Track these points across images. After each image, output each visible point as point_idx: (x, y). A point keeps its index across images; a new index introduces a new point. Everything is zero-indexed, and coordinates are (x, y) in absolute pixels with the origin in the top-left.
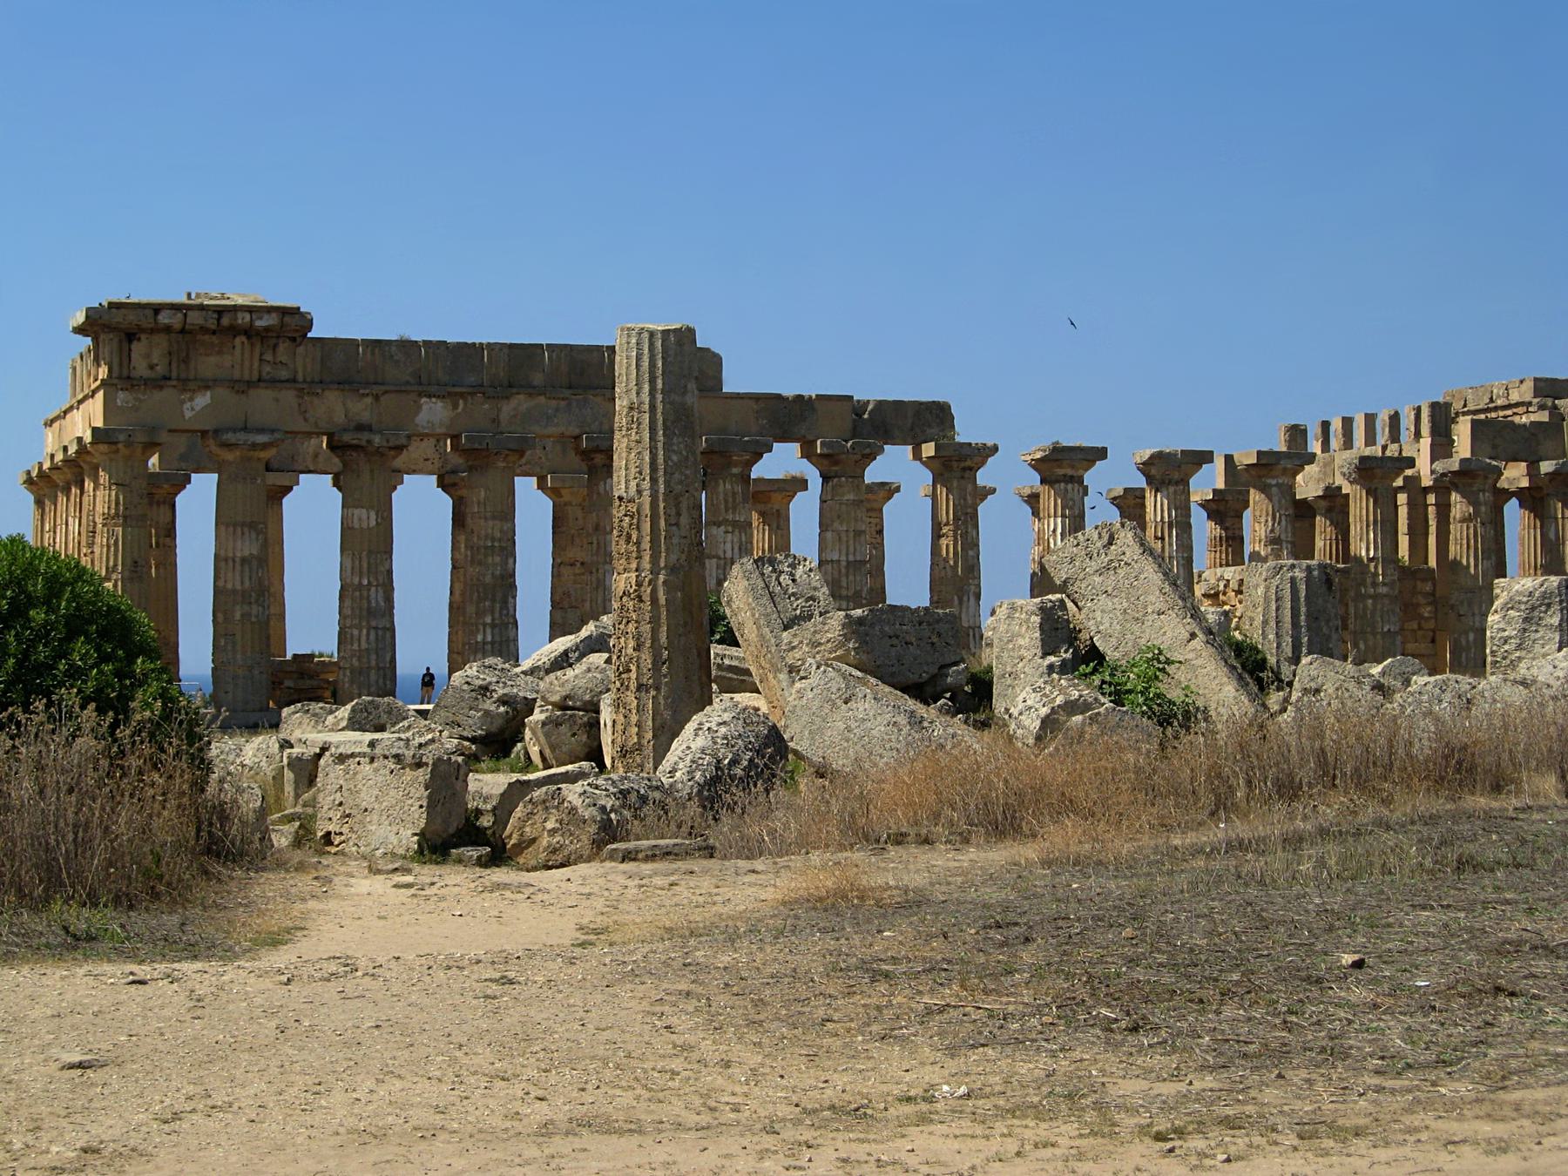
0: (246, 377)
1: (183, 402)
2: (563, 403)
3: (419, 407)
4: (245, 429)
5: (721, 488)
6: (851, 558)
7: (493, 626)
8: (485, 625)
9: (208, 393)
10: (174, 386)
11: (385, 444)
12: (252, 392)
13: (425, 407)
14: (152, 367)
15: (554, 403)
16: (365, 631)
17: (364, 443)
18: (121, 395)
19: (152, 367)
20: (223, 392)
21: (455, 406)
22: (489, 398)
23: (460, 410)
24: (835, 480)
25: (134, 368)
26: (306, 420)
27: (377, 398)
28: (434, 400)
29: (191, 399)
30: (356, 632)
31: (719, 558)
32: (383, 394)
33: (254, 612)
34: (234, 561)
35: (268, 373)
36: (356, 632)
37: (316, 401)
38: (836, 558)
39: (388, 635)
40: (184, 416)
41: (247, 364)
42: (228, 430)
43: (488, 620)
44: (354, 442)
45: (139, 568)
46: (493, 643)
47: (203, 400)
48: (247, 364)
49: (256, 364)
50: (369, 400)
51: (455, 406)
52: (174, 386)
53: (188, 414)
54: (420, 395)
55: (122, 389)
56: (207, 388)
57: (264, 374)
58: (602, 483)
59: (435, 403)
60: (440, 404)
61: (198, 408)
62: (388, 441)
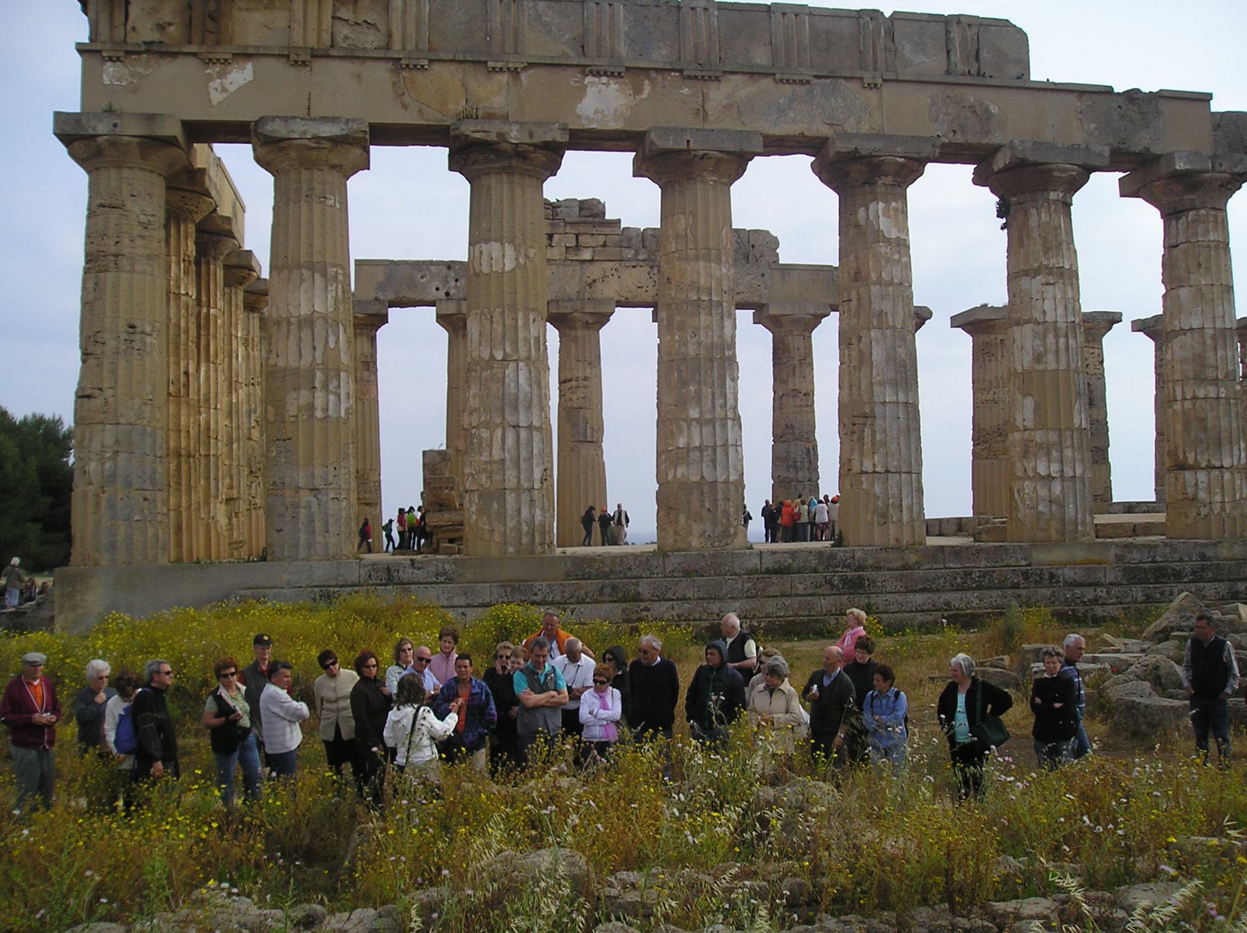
0: (312, 42)
1: (210, 78)
2: (804, 88)
3: (583, 90)
4: (308, 117)
5: (1033, 221)
6: (1219, 325)
7: (700, 422)
8: (689, 422)
9: (249, 66)
10: (194, 54)
11: (528, 141)
12: (318, 65)
13: (591, 91)
14: (162, 27)
15: (788, 88)
16: (499, 432)
17: (493, 137)
18: (110, 68)
19: (162, 27)
20: (275, 67)
21: (638, 90)
22: (689, 77)
23: (645, 95)
24: (1192, 213)
25: (134, 29)
26: (405, 107)
27: (515, 73)
28: (604, 79)
29: (221, 75)
30: (485, 434)
31: (1038, 323)
32: (525, 68)
33: (319, 403)
34: (289, 323)
35: (346, 38)
36: (485, 434)
37: (420, 77)
38: (1196, 323)
39: (537, 437)
40: (210, 100)
41: (313, 23)
42: (273, 119)
43: (694, 413)
44: (478, 135)
45: (136, 337)
46: (701, 449)
47: (241, 75)
48: (313, 23)
49: (327, 20)
50: (504, 78)
51: (638, 90)
52: (194, 54)
53: (216, 97)
54: (585, 70)
55: (110, 59)
56: (248, 56)
57: (339, 39)
58: (862, 211)
59: (607, 85)
60: (614, 86)
61: (232, 88)
62: (531, 135)
